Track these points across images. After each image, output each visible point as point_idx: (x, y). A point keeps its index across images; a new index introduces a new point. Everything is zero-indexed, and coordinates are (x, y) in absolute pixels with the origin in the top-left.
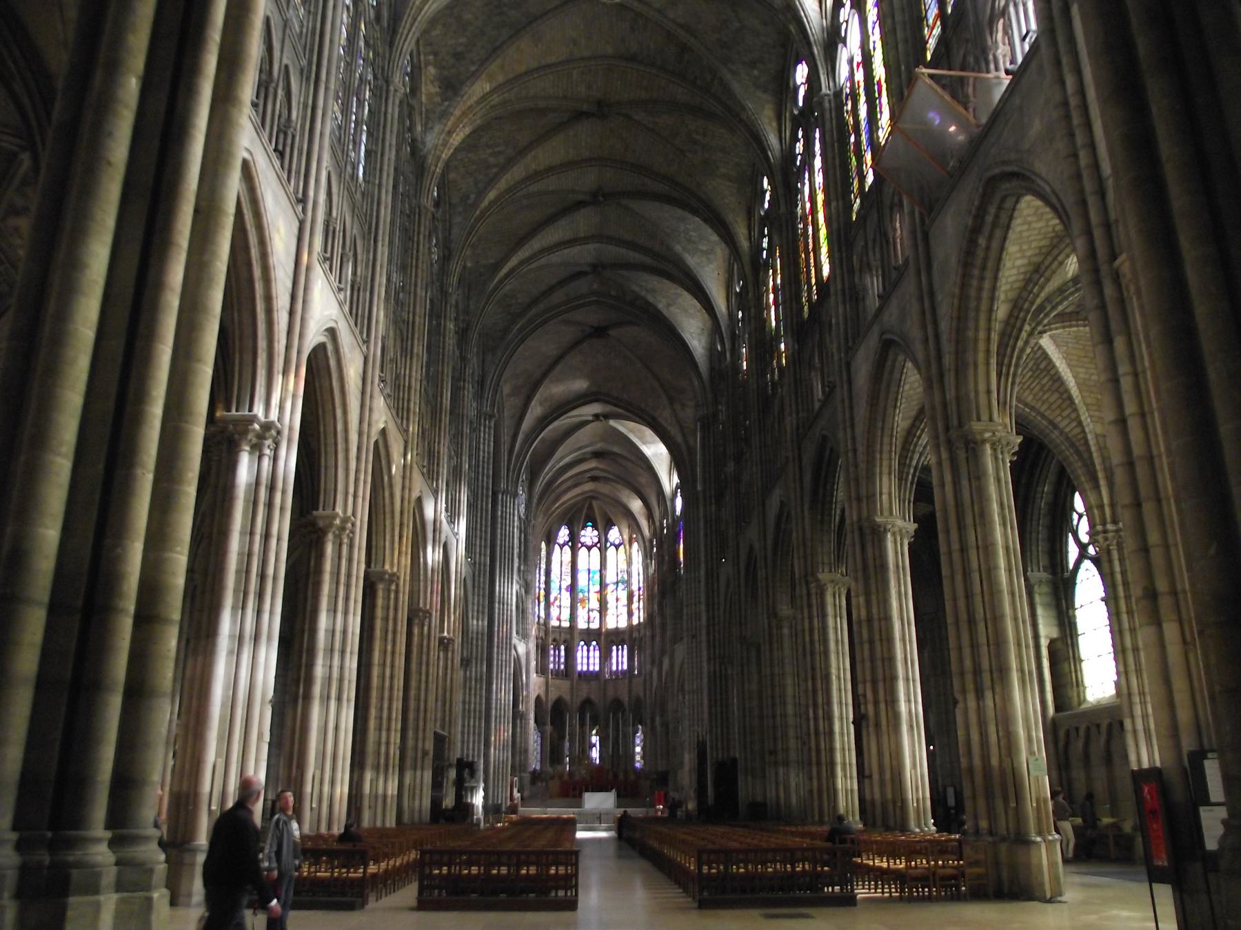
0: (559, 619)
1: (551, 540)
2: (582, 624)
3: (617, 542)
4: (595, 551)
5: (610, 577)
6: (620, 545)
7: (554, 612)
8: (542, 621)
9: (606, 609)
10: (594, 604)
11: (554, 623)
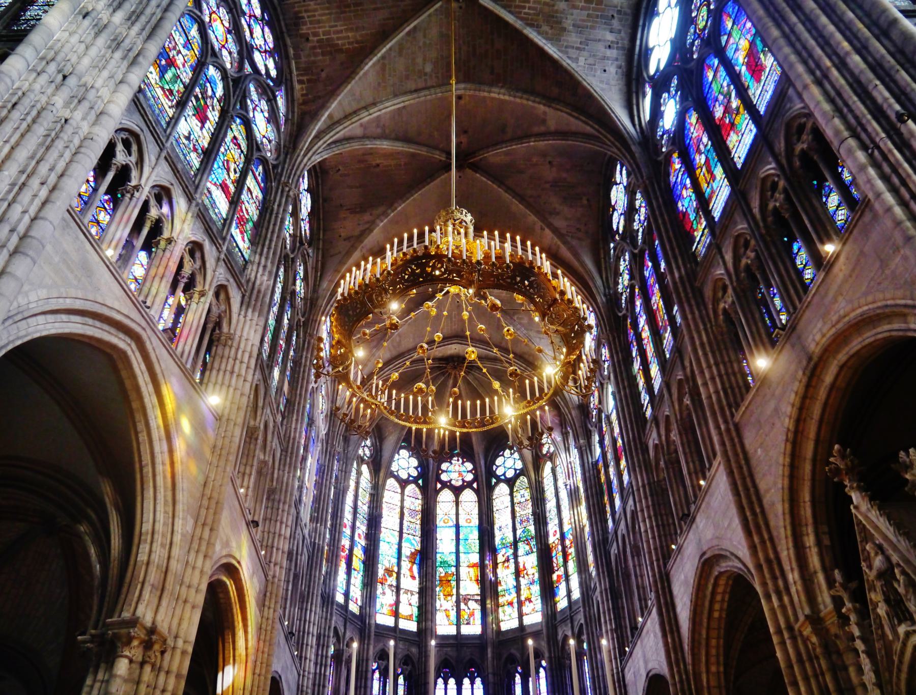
0: (396, 614)
1: (379, 466)
2: (444, 626)
3: (510, 474)
4: (469, 496)
5: (503, 531)
6: (517, 476)
7: (385, 598)
8: (354, 608)
9: (496, 595)
10: (470, 587)
11: (384, 619)
